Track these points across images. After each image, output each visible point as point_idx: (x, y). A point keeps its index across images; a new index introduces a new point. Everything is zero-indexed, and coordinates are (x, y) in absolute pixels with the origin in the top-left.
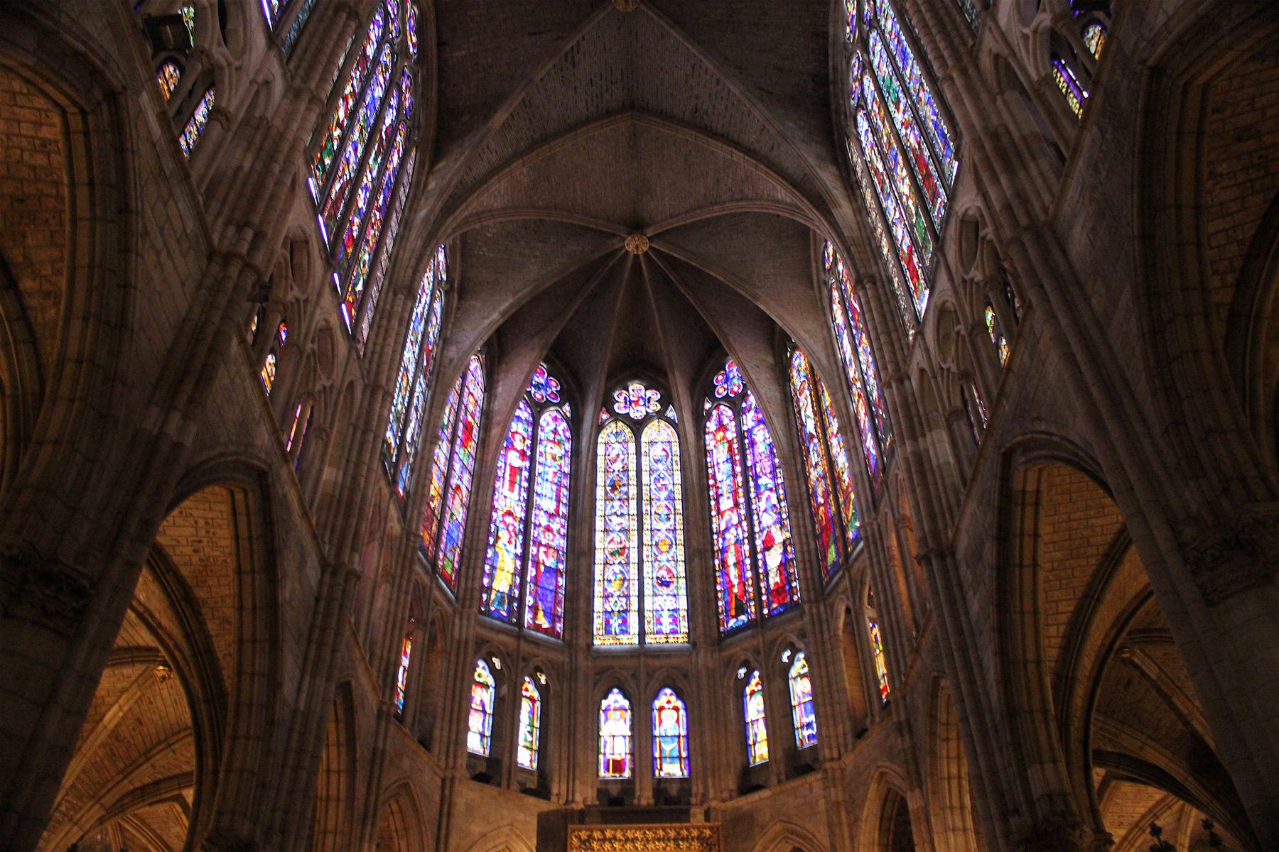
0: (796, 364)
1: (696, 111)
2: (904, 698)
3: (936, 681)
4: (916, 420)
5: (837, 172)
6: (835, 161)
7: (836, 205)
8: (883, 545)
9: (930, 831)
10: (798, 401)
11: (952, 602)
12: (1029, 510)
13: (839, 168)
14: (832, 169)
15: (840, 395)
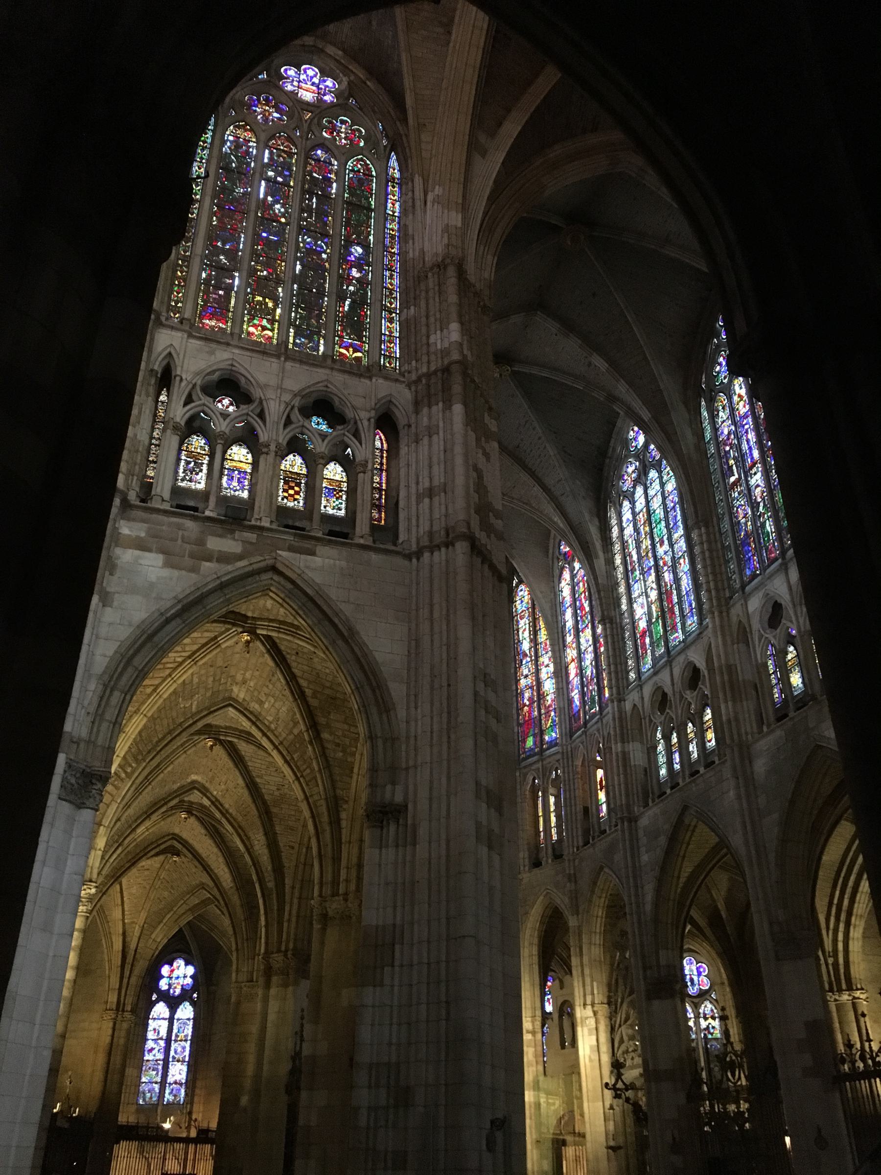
0: (520, 594)
1: (518, 447)
2: (574, 860)
3: (601, 868)
4: (625, 731)
5: (597, 523)
6: (598, 516)
7: (597, 557)
8: (573, 761)
9: (580, 940)
10: (518, 622)
11: (632, 849)
12: (689, 833)
13: (600, 521)
14: (597, 522)
15: (557, 648)
